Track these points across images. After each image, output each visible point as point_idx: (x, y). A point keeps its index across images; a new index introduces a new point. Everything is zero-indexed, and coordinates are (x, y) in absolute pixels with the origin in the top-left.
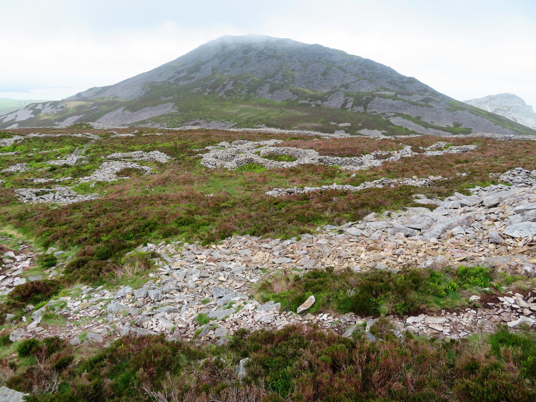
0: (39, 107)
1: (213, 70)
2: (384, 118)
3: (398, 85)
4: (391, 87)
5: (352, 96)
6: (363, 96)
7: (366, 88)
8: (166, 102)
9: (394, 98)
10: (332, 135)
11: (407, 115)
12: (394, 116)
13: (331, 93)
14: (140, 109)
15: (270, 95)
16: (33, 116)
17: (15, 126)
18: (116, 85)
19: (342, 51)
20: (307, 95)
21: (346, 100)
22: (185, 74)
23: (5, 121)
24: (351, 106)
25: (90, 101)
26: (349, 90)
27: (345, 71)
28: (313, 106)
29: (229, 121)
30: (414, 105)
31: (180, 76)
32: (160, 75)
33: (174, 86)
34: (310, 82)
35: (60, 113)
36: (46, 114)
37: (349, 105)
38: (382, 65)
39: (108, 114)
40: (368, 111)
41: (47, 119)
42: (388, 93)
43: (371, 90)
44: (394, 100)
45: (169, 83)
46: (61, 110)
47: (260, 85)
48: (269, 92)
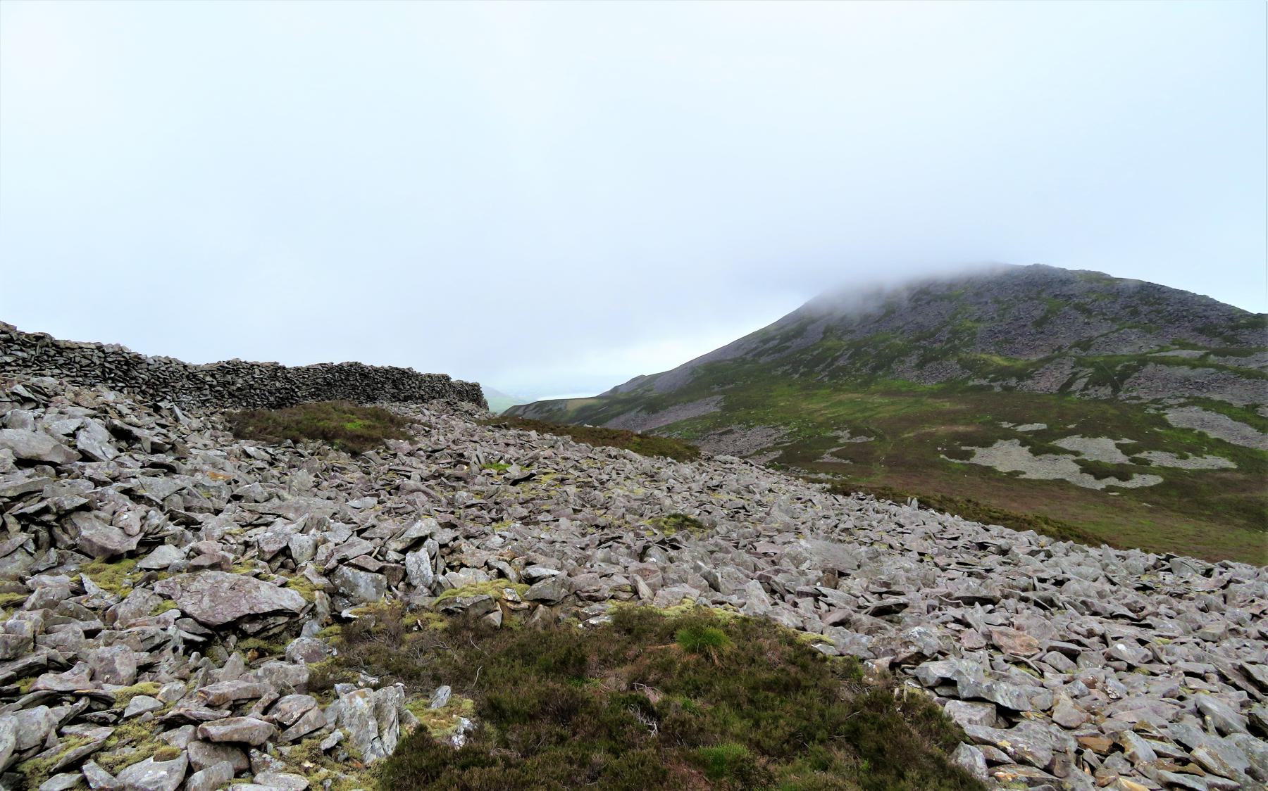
1: (824, 333)
2: (1152, 411)
3: (1221, 333)
4: (1202, 340)
5: (1092, 364)
6: (1118, 363)
8: (713, 394)
9: (1201, 362)
11: (1222, 402)
12: (1181, 405)
13: (1048, 360)
15: (915, 373)
19: (1098, 274)
21: (1076, 374)
22: (775, 342)
24: (1082, 386)
26: (1090, 352)
27: (1088, 312)
28: (998, 389)
29: (786, 425)
30: (1249, 378)
31: (767, 346)
32: (738, 348)
37: (1080, 384)
38: (1182, 292)
40: (1122, 395)
42: (1185, 354)
44: (1194, 367)
45: (744, 360)
47: (903, 353)
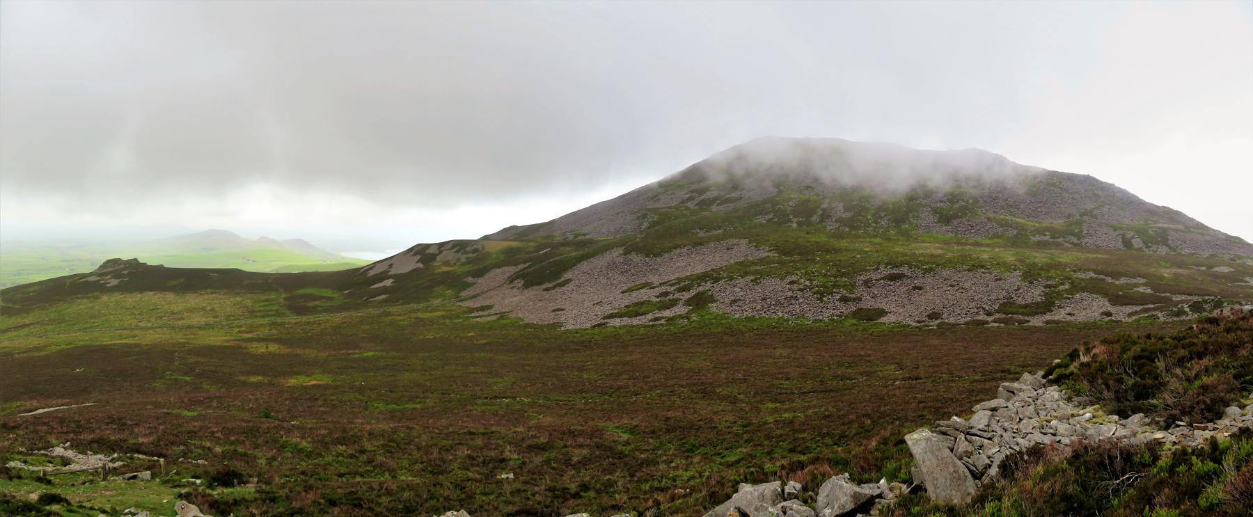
0: (430, 251)
10: (1048, 317)
16: (420, 265)
17: (388, 283)
18: (552, 222)
23: (371, 273)
33: (705, 214)
35: (475, 261)
36: (447, 263)
39: (585, 263)
41: (448, 272)
45: (687, 209)
48: (939, 221)
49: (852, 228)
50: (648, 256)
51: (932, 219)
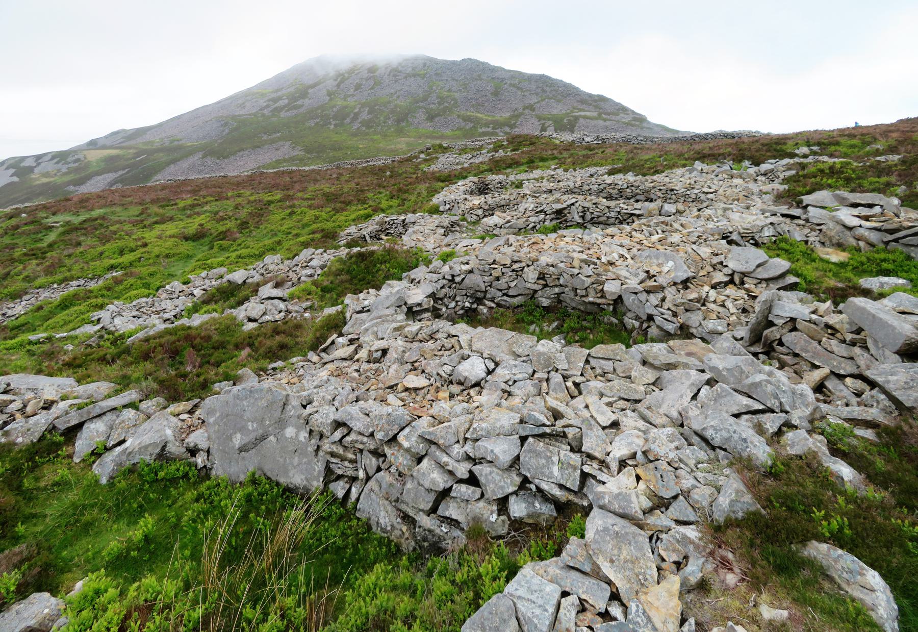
4: (584, 107)
7: (558, 110)
8: (272, 142)
14: (234, 153)
20: (484, 122)
25: (130, 148)
32: (242, 106)
34: (479, 105)
39: (173, 166)
41: (50, 182)
43: (564, 112)
45: (263, 115)
46: (77, 164)
48: (427, 119)
49: (368, 127)
50: (218, 158)
51: (424, 117)
